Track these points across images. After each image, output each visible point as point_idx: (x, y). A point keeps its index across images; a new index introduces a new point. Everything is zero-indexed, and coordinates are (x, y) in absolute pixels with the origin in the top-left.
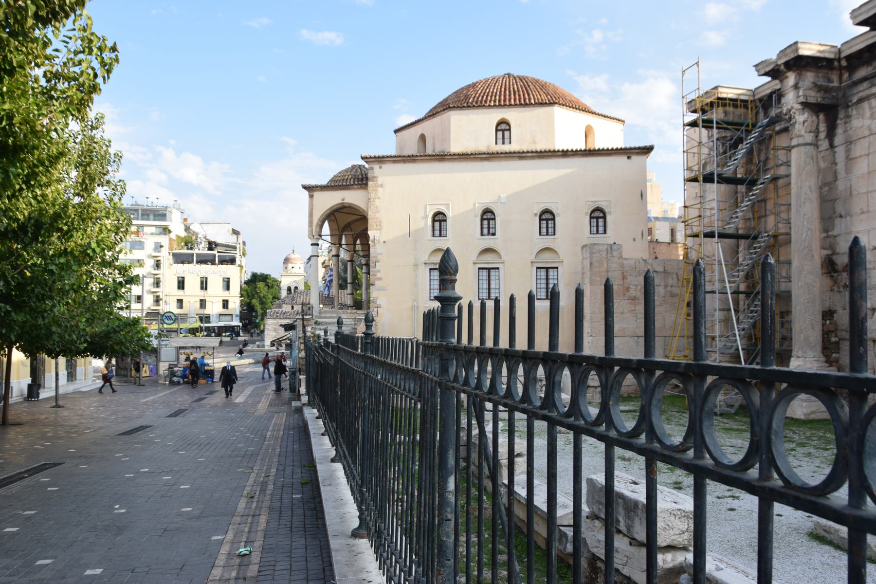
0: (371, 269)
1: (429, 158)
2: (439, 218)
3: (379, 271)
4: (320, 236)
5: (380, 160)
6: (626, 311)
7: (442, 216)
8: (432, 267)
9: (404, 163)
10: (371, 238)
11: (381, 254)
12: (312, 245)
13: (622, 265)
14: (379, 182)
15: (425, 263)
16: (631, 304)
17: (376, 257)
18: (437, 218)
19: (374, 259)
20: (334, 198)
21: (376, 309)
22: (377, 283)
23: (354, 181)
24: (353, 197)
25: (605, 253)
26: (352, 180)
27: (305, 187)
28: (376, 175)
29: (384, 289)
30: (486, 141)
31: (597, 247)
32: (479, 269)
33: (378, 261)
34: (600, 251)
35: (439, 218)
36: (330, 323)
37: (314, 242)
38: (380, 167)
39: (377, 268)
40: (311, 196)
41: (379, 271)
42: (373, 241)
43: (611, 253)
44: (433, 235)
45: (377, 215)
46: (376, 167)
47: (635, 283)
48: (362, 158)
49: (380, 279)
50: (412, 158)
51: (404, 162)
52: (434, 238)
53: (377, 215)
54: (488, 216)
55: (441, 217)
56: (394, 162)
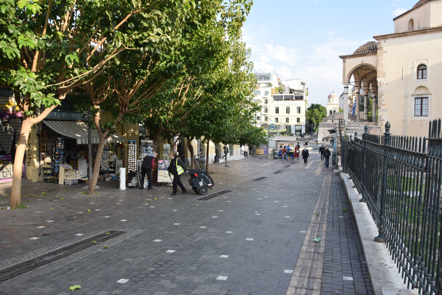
0: (379, 100)
1: (416, 32)
2: (422, 68)
3: (383, 100)
4: (349, 83)
5: (385, 37)
7: (424, 66)
8: (417, 97)
9: (400, 37)
10: (379, 82)
11: (385, 91)
12: (345, 88)
14: (384, 50)
15: (412, 95)
17: (382, 93)
18: (420, 68)
19: (381, 94)
20: (357, 61)
21: (381, 122)
22: (382, 107)
23: (369, 51)
24: (368, 60)
26: (368, 50)
27: (341, 57)
28: (382, 46)
29: (386, 110)
33: (383, 95)
35: (422, 68)
37: (346, 86)
38: (385, 41)
39: (382, 99)
40: (344, 62)
41: (383, 100)
42: (380, 84)
44: (418, 78)
45: (383, 69)
46: (382, 41)
48: (374, 37)
49: (384, 105)
50: (405, 34)
51: (400, 37)
52: (418, 80)
53: (383, 69)
55: (423, 67)
56: (393, 37)
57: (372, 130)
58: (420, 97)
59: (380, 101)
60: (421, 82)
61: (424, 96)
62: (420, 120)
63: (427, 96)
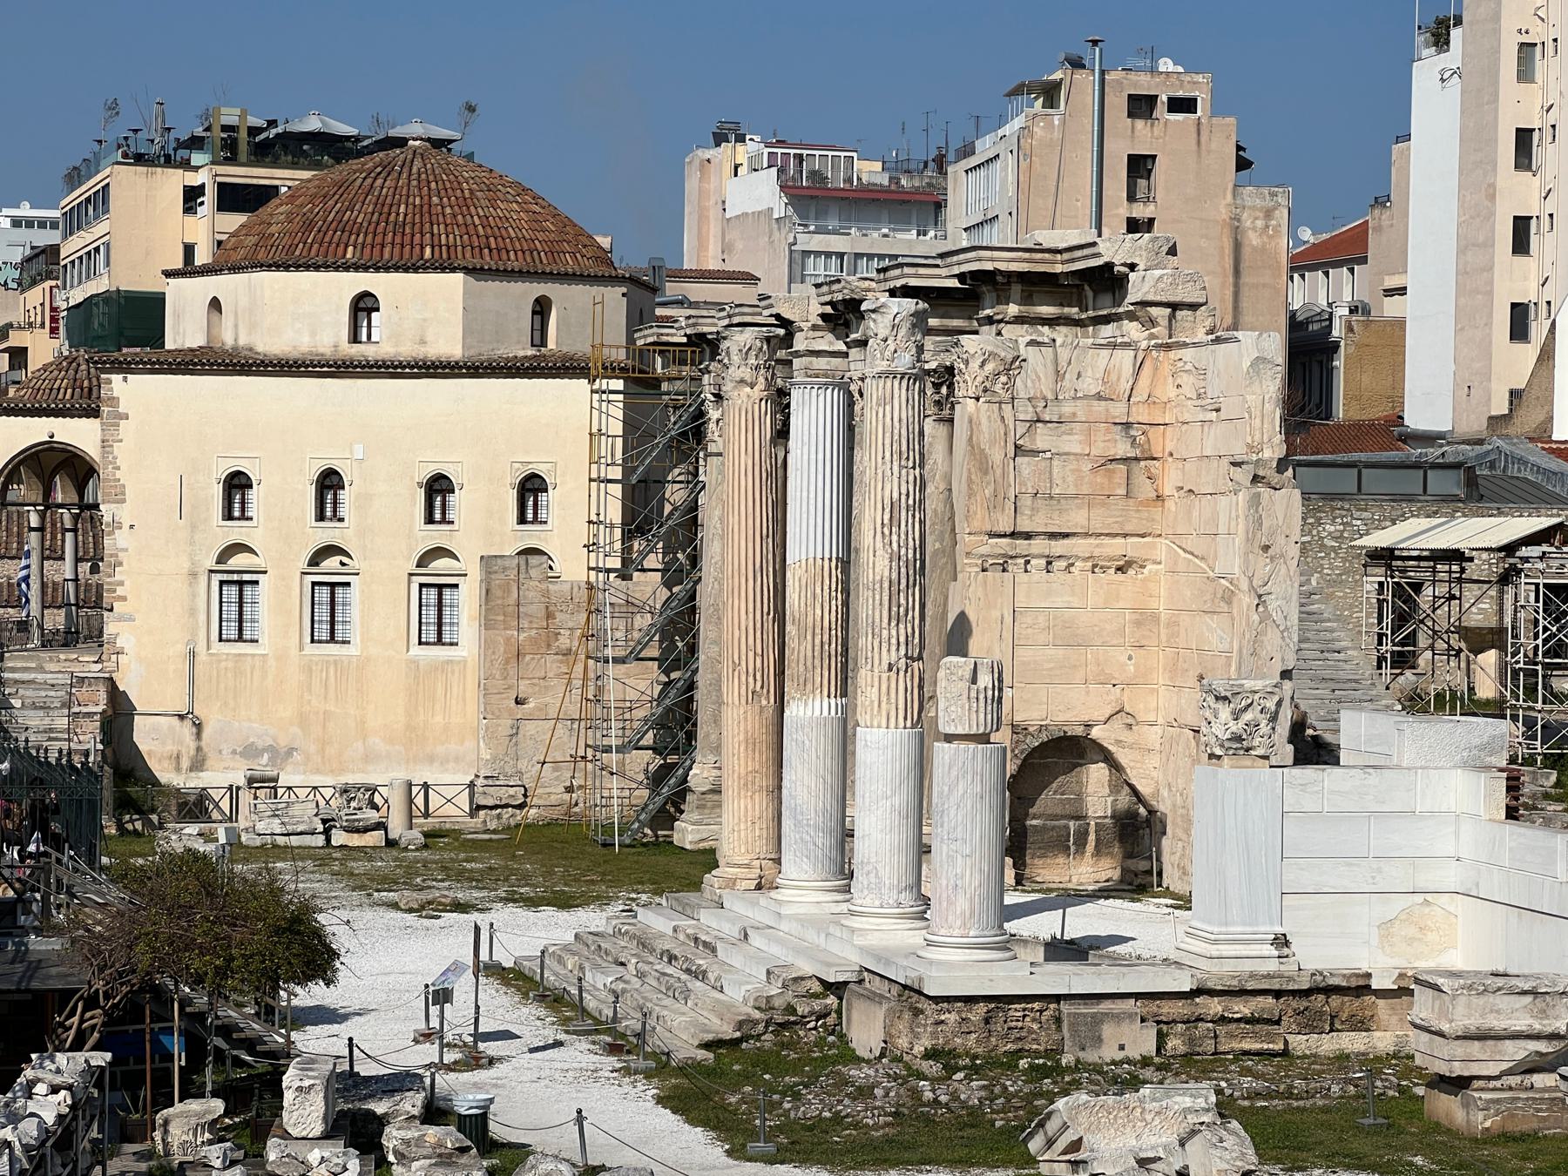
2: (237, 484)
3: (121, 583)
6: (550, 675)
8: (225, 577)
10: (107, 519)
11: (126, 550)
13: (546, 594)
16: (561, 662)
21: (114, 657)
25: (516, 572)
29: (131, 619)
30: (331, 337)
31: (499, 561)
32: (314, 584)
33: (121, 564)
34: (505, 569)
35: (237, 484)
36: (23, 682)
38: (125, 379)
39: (118, 577)
41: (121, 583)
43: (527, 572)
45: (118, 474)
46: (116, 379)
47: (571, 625)
49: (124, 599)
54: (329, 482)
57: (84, 689)
58: (235, 577)
59: (109, 583)
60: (235, 532)
61: (246, 577)
62: (236, 655)
63: (254, 577)
